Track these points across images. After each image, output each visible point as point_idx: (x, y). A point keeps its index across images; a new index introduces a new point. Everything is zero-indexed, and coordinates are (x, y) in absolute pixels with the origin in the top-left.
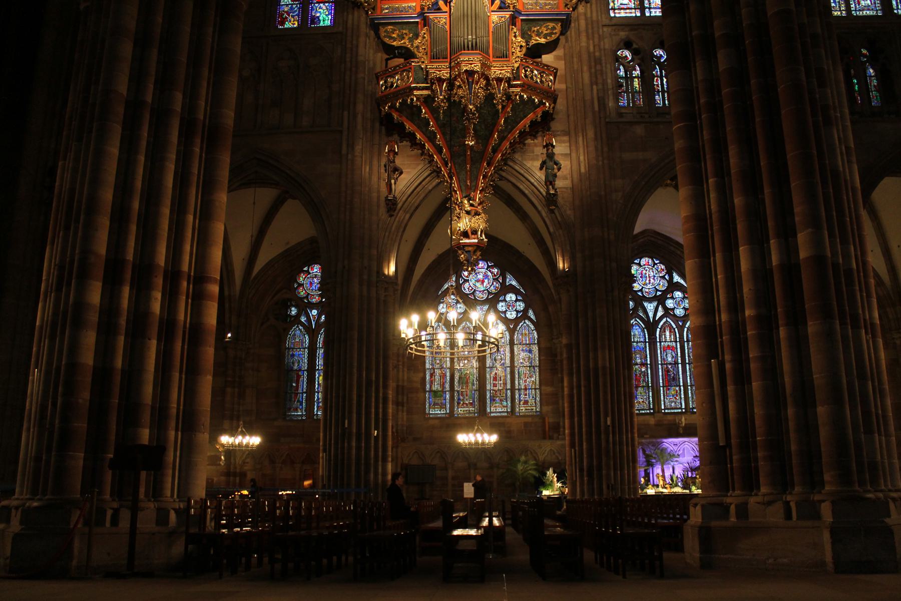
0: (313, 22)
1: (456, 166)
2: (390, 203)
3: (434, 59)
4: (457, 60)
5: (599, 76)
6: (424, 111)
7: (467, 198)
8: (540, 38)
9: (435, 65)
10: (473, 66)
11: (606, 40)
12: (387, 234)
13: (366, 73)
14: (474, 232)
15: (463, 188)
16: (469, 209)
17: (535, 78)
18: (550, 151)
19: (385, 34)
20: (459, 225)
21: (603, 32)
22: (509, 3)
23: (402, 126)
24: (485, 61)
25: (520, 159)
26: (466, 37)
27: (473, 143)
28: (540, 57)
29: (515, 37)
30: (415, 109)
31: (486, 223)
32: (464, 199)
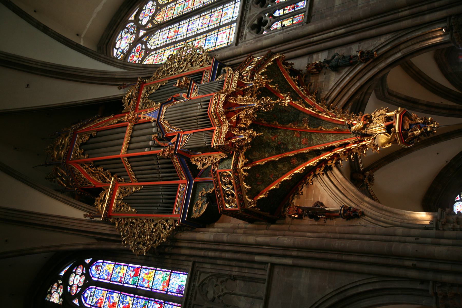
10: (220, 102)
25: (326, 93)
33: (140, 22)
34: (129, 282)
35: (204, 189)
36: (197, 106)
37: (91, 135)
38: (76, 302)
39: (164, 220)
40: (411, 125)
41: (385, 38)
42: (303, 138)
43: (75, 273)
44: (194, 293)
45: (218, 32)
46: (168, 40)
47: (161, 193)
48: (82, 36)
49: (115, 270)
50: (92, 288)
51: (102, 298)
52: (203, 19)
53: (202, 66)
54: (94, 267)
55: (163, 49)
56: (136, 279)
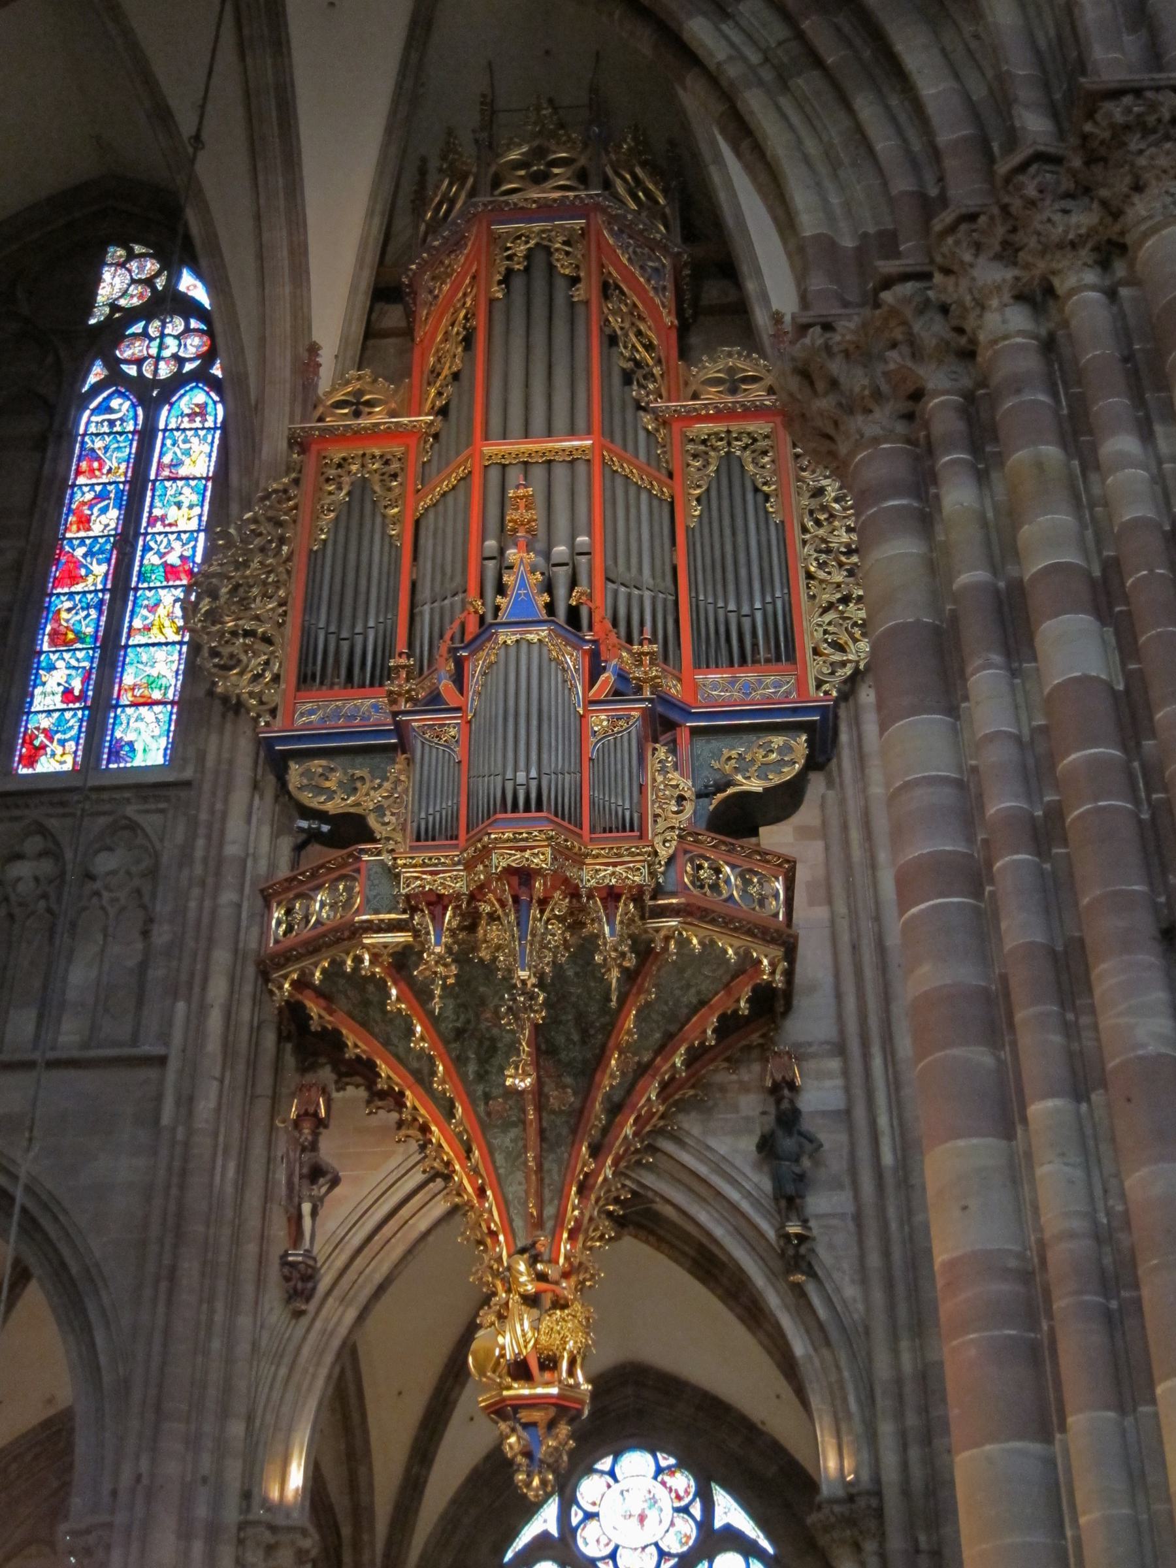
0: (115, 754)
1: (499, 1158)
2: (296, 1275)
3: (418, 839)
4: (480, 840)
6: (394, 992)
7: (526, 1256)
8: (748, 778)
9: (420, 856)
10: (527, 854)
12: (283, 1371)
14: (549, 1363)
15: (518, 1223)
16: (530, 1288)
18: (785, 1105)
19: (305, 781)
20: (500, 1340)
22: (638, 679)
23: (332, 1041)
24: (566, 841)
25: (696, 1131)
26: (509, 775)
27: (528, 1081)
28: (755, 833)
29: (663, 770)
30: (371, 988)
31: (588, 1334)
32: (517, 1257)
34: (149, 555)
35: (378, 781)
36: (528, 772)
38: (97, 373)
39: (280, 666)
41: (855, 1300)
42: (505, 1102)
43: (188, 330)
44: (107, 807)
47: (371, 623)
49: (189, 485)
51: (105, 471)
53: (816, 652)
56: (157, 579)
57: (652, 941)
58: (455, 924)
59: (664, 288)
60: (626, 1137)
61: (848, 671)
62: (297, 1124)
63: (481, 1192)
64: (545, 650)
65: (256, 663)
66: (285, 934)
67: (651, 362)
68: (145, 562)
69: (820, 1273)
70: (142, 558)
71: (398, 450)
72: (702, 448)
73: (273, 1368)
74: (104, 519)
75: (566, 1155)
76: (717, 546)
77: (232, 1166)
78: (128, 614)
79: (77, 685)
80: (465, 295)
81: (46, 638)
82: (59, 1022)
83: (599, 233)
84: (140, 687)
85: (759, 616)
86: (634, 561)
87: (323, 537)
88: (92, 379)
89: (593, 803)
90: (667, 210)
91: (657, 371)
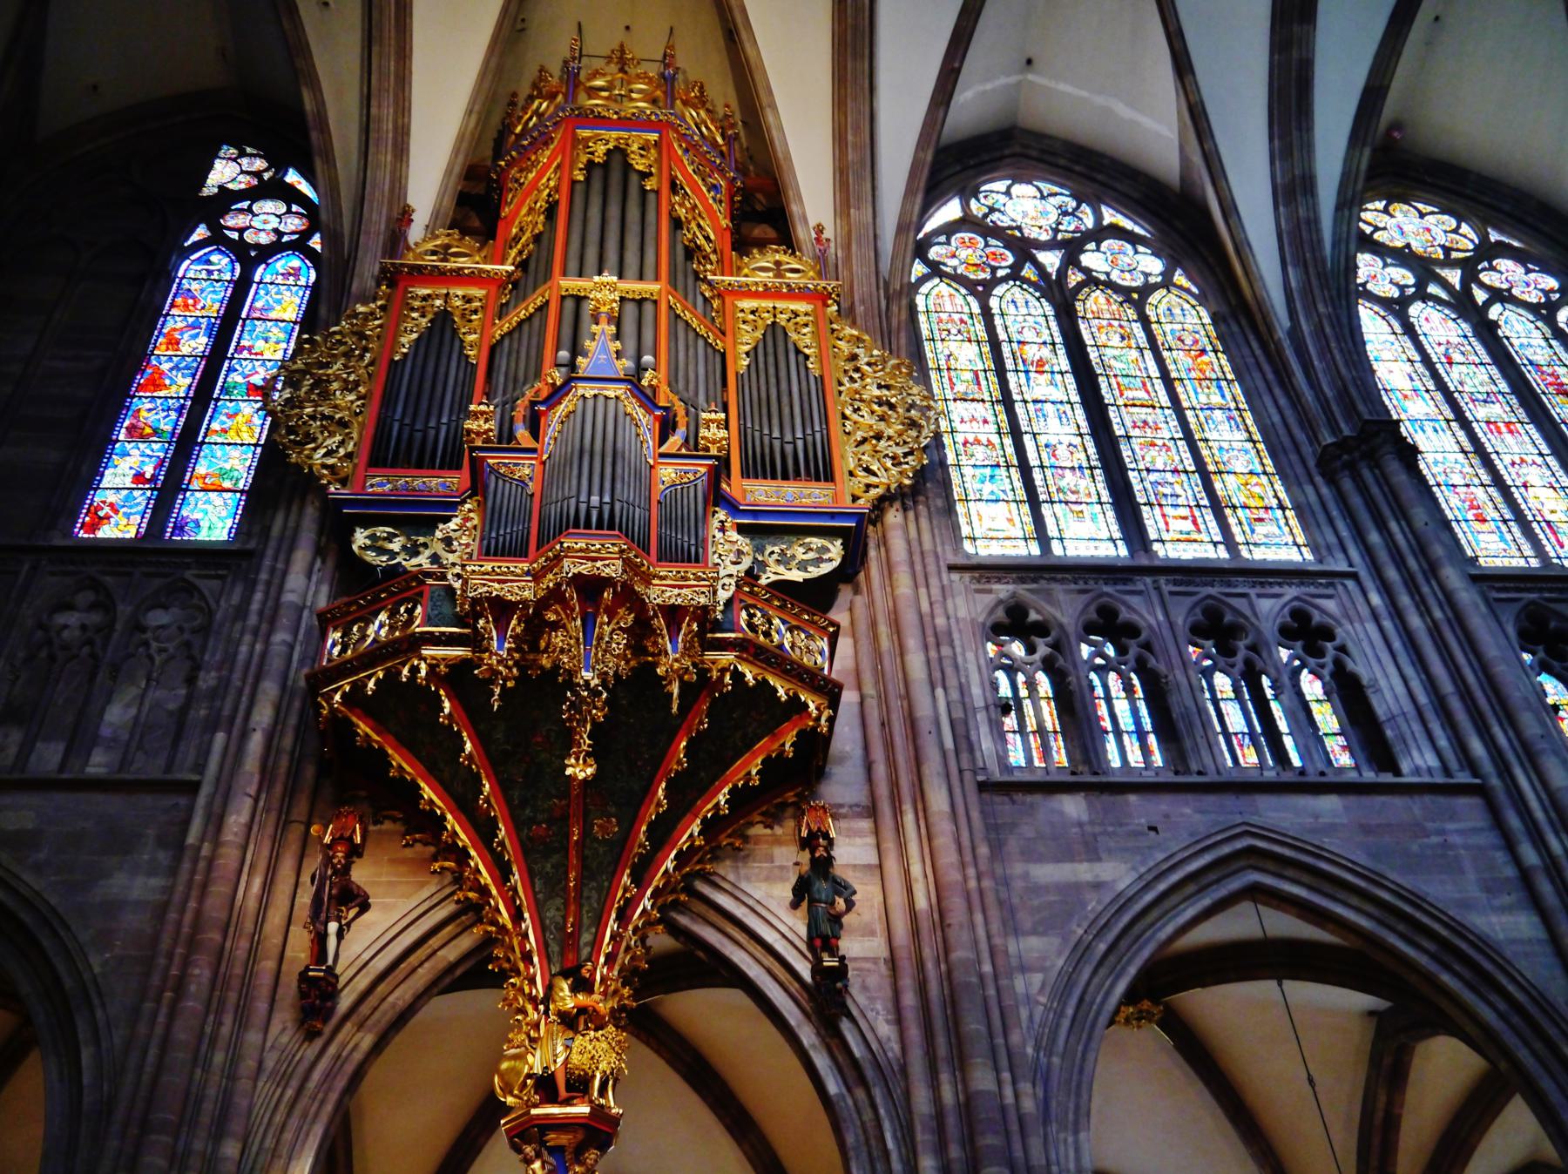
0: (180, 528)
3: (488, 554)
5: (949, 671)
10: (599, 564)
11: (960, 600)
12: (290, 1093)
13: (301, 637)
14: (579, 1085)
17: (776, 637)
18: (820, 852)
19: (368, 542)
21: (951, 581)
24: (636, 556)
25: (731, 877)
26: (583, 498)
29: (722, 529)
33: (1092, 246)
34: (233, 375)
36: (601, 497)
37: (651, 174)
38: (201, 232)
40: (557, 1151)
41: (889, 1039)
42: (548, 829)
43: (289, 211)
45: (1015, 501)
46: (1015, 345)
47: (444, 420)
48: (1030, 77)
49: (277, 326)
50: (233, 270)
51: (199, 307)
52: (1070, 445)
54: (295, 262)
55: (983, 335)
57: (710, 670)
58: (518, 630)
59: (721, 202)
60: (667, 871)
61: (880, 491)
62: (329, 846)
63: (517, 917)
64: (620, 405)
65: (332, 442)
66: (339, 655)
67: (708, 250)
68: (229, 379)
69: (855, 1012)
70: (227, 376)
71: (478, 292)
72: (752, 317)
73: (279, 1090)
74: (193, 343)
75: (606, 884)
76: (763, 388)
77: (257, 883)
78: (207, 418)
79: (149, 471)
80: (549, 180)
81: (123, 430)
82: (89, 755)
83: (670, 146)
84: (212, 475)
85: (800, 444)
86: (692, 387)
87: (405, 350)
88: (195, 237)
89: (660, 538)
90: (724, 148)
91: (713, 257)
